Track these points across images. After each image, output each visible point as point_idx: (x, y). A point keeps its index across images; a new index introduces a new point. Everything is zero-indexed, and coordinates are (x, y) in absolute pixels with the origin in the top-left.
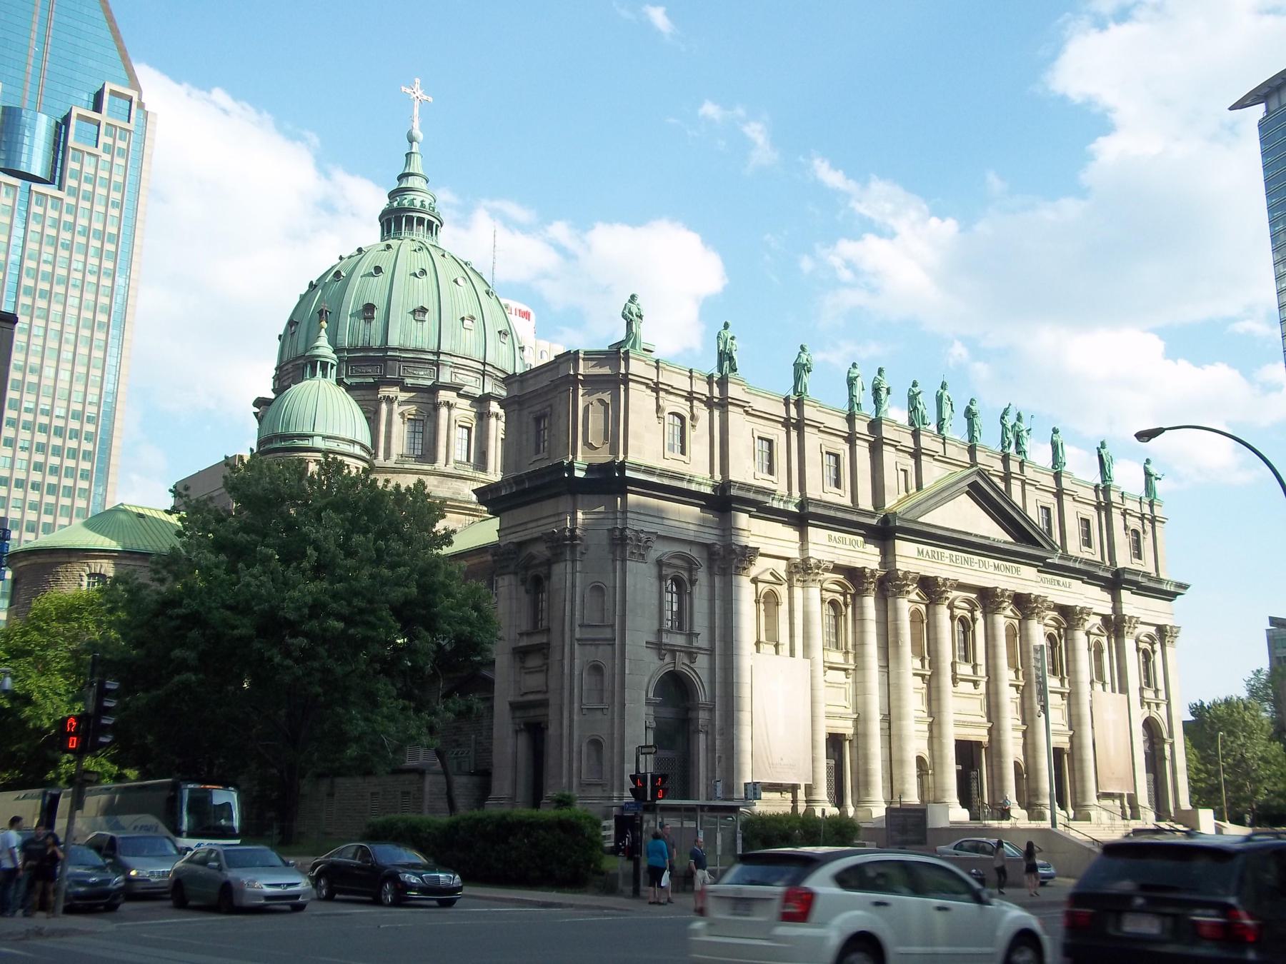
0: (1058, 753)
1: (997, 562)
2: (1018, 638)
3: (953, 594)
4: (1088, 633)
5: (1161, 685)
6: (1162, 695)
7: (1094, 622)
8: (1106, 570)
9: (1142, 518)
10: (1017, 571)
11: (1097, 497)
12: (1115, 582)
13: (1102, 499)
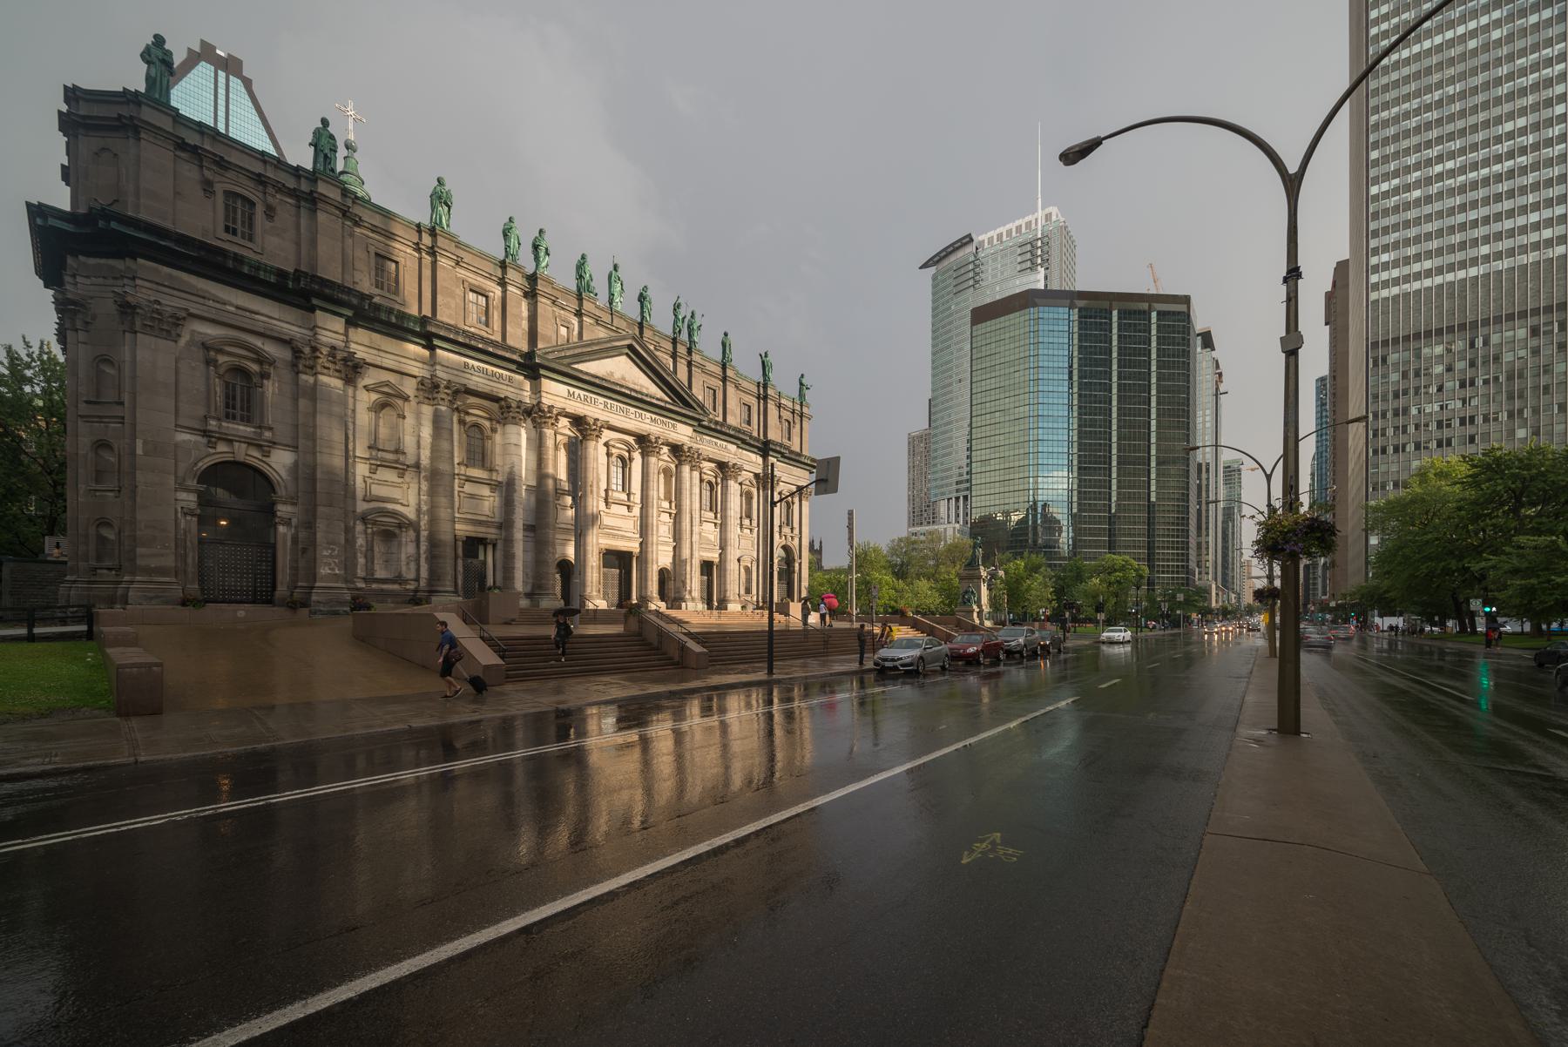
0: (707, 567)
1: (654, 416)
2: (674, 479)
3: (607, 435)
4: (741, 484)
5: (796, 525)
6: (796, 531)
7: (746, 476)
8: (757, 440)
9: (793, 412)
10: (673, 426)
11: (759, 391)
12: (765, 449)
13: (762, 392)
